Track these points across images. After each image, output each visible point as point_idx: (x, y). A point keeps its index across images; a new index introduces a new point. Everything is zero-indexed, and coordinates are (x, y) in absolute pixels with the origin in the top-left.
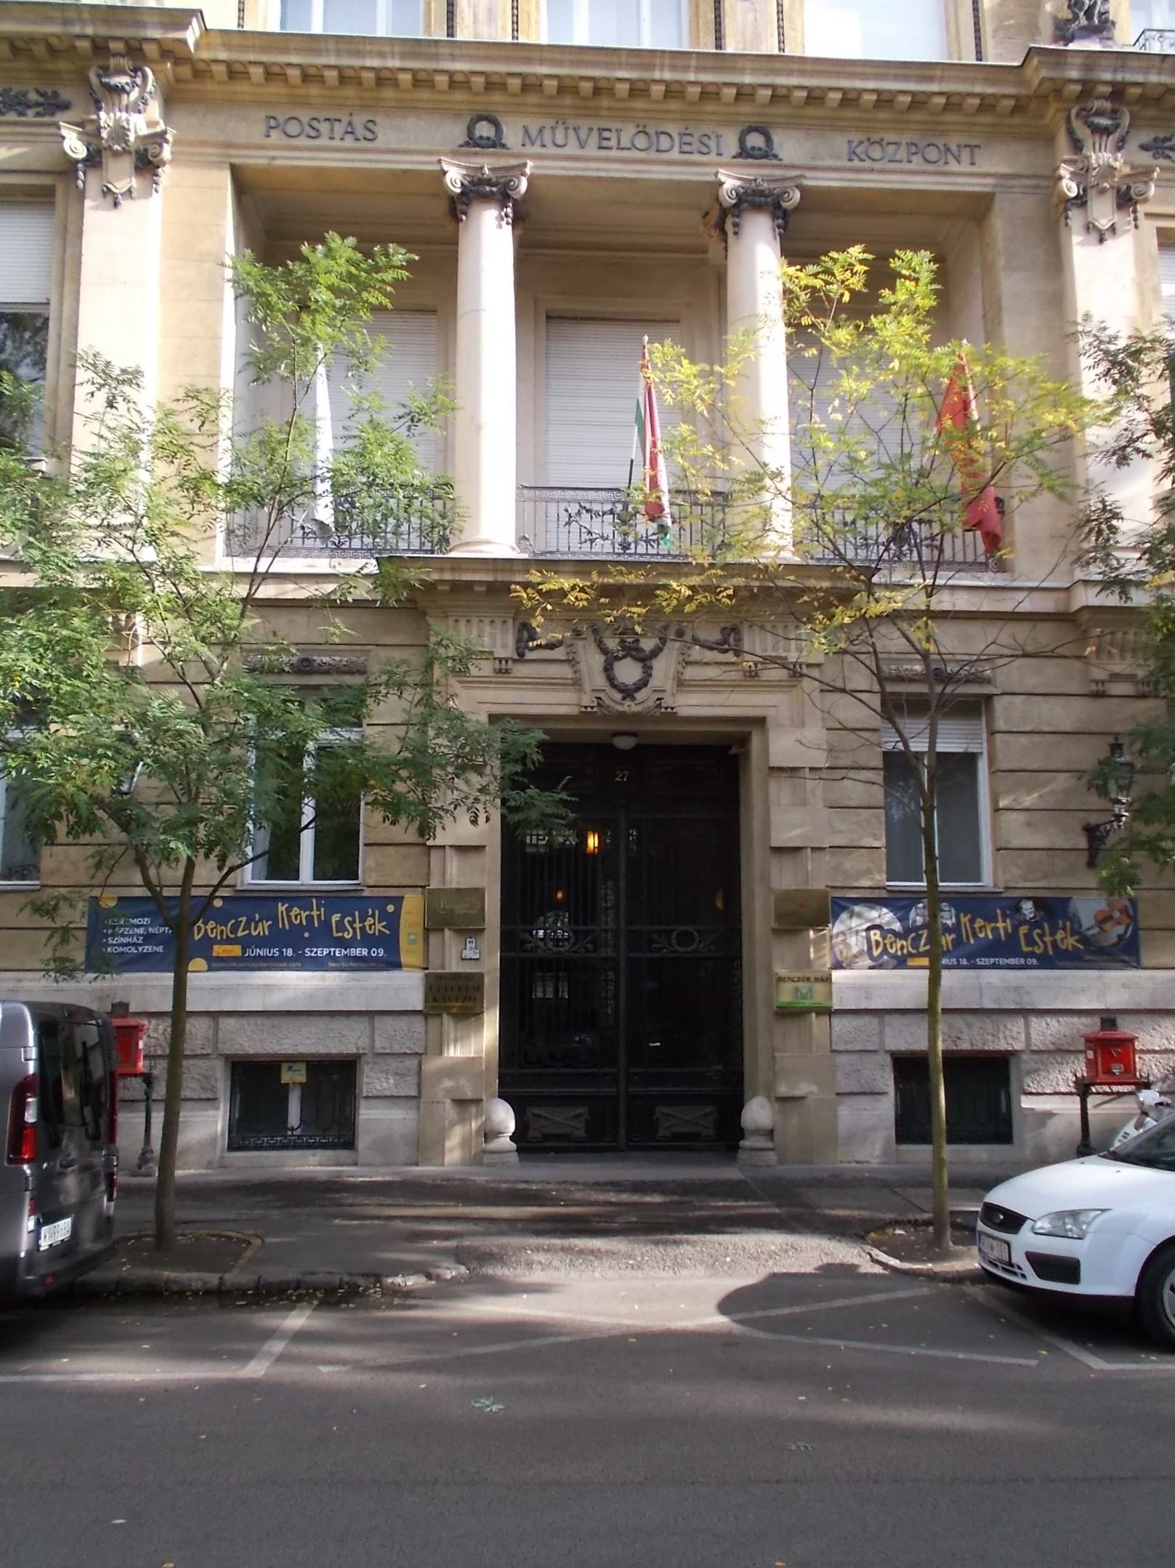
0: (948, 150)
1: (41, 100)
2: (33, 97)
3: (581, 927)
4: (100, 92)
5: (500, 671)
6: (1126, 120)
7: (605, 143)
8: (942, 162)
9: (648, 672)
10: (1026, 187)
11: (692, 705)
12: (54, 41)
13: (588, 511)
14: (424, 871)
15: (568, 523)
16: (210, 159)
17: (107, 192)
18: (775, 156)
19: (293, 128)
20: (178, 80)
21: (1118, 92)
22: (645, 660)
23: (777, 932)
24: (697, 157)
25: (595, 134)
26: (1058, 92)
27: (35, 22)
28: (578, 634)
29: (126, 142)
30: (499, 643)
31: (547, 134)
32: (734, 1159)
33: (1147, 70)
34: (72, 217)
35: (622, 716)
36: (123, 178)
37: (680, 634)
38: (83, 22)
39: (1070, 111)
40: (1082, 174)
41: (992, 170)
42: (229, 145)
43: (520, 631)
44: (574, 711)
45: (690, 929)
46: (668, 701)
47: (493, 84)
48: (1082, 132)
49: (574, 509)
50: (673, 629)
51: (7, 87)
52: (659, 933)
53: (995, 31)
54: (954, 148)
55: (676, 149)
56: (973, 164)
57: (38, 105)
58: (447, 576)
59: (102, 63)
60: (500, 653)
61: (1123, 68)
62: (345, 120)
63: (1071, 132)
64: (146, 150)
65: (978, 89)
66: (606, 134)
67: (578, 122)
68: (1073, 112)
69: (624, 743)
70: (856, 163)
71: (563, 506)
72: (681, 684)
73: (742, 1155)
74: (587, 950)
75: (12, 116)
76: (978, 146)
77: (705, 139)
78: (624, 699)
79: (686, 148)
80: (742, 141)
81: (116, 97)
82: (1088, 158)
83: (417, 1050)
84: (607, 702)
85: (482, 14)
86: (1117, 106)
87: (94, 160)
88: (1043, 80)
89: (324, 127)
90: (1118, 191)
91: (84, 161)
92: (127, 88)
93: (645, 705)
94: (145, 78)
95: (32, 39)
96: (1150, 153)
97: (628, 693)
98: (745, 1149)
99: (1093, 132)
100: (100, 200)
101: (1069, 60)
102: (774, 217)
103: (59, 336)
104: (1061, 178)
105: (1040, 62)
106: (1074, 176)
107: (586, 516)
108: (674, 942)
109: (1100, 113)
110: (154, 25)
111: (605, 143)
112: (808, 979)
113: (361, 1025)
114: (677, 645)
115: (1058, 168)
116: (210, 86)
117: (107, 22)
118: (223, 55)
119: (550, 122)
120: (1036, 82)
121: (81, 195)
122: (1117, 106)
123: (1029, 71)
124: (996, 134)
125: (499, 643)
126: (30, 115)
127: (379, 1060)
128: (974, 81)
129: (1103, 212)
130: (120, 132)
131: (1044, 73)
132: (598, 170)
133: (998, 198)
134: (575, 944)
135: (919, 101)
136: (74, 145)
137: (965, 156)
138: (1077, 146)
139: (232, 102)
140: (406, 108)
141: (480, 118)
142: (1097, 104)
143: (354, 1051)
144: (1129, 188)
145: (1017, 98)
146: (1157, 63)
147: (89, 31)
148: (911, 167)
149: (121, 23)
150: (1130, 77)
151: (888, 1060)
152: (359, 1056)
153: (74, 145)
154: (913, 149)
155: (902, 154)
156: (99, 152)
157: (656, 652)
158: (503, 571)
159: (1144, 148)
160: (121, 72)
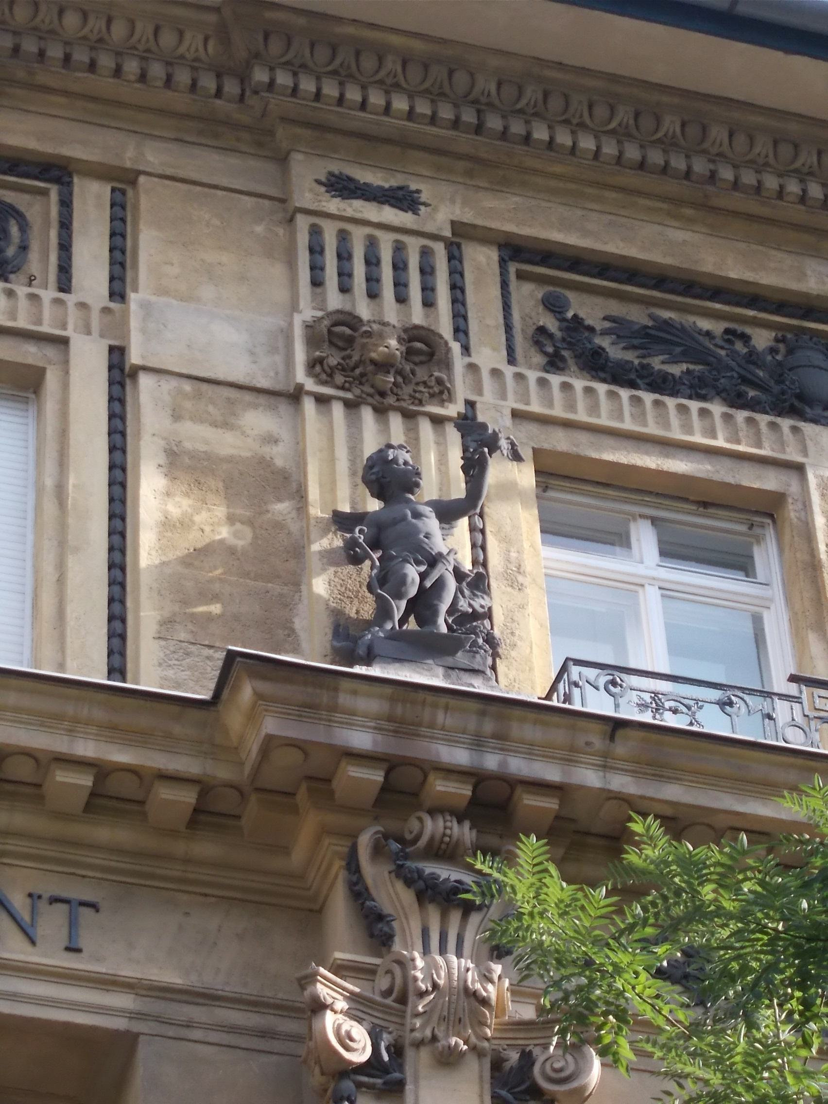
10: (233, 1029)
26: (321, 785)
33: (570, 756)
39: (353, 836)
40: (387, 1003)
41: (128, 972)
48: (392, 895)
53: (168, 623)
56: (73, 949)
63: (359, 893)
65: (86, 748)
68: (365, 841)
76: (93, 906)
82: (404, 964)
88: (269, 743)
90: (497, 1065)
99: (421, 897)
101: (344, 699)
104: (319, 1007)
105: (259, 696)
106: (359, 1007)
115: (311, 978)
120: (253, 747)
123: (234, 718)
124: (144, 879)
128: (74, 726)
131: (271, 725)
133: (144, 1052)
137: (52, 924)
138: (377, 930)
142: (432, 827)
144: (527, 1059)
145: (205, 787)
146: (596, 738)
150: (518, 765)
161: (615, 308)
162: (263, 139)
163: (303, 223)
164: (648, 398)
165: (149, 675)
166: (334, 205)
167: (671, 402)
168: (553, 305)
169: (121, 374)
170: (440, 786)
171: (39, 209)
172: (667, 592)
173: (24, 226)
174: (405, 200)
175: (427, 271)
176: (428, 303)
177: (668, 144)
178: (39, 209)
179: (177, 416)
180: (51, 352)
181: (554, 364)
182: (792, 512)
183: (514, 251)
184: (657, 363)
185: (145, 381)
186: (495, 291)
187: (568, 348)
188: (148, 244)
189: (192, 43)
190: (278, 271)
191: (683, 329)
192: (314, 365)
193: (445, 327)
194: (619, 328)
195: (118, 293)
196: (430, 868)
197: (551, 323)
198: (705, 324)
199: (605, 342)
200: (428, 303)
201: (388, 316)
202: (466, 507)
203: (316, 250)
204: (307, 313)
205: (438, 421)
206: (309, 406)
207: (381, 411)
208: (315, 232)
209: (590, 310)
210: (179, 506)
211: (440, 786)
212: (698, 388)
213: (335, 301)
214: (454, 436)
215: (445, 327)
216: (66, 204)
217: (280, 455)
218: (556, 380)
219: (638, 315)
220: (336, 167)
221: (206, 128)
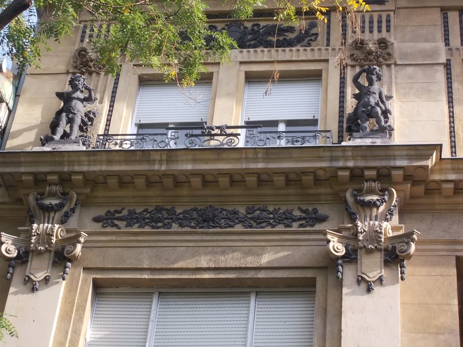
1: (304, 215)
2: (297, 213)
4: (353, 209)
12: (320, 173)
16: (440, 253)
17: (360, 280)
20: (412, 197)
27: (308, 161)
29: (379, 242)
34: (330, 301)
36: (372, 267)
38: (346, 159)
42: (455, 242)
51: (277, 207)
57: (300, 219)
59: (357, 186)
64: (394, 248)
75: (281, 228)
87: (351, 257)
91: (343, 257)
92: (378, 203)
94: (391, 195)
95: (304, 172)
100: (356, 287)
110: (402, 157)
116: (437, 199)
117: (365, 157)
118: (452, 177)
121: (340, 284)
126: (295, 226)
130: (375, 235)
136: (336, 246)
139: (454, 210)
147: (350, 164)
149: (375, 158)
153: (336, 246)
156: (355, 251)
160: (371, 192)
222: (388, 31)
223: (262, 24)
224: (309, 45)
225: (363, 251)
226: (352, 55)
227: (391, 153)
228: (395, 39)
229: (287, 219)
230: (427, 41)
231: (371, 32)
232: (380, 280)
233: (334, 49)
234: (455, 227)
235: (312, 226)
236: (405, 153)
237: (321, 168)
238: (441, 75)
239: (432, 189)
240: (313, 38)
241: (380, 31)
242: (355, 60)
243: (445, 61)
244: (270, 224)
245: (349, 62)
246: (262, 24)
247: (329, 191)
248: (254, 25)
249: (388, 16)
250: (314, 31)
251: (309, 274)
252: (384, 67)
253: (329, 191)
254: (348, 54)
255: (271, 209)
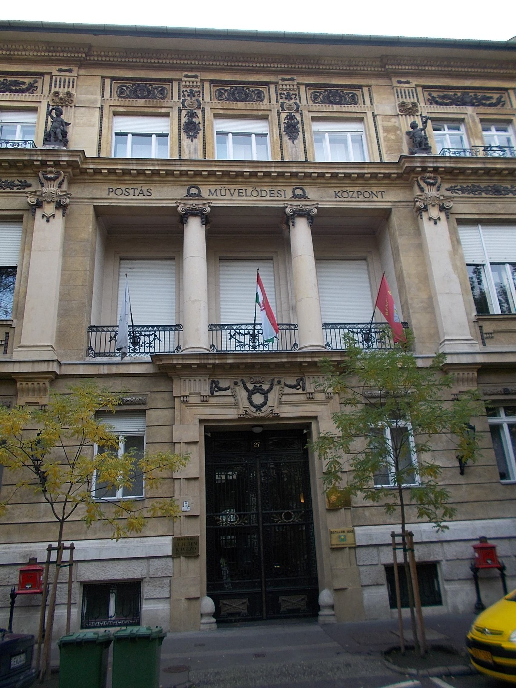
0: (372, 193)
1: (20, 183)
3: (242, 513)
4: (43, 180)
5: (203, 401)
6: (439, 180)
7: (241, 194)
8: (371, 197)
9: (266, 399)
11: (286, 412)
12: (26, 162)
13: (238, 333)
14: (172, 490)
15: (230, 339)
18: (307, 197)
19: (119, 192)
20: (74, 175)
21: (436, 170)
22: (265, 394)
23: (329, 510)
24: (277, 198)
25: (237, 191)
28: (236, 383)
30: (202, 389)
31: (218, 192)
32: (317, 621)
35: (256, 419)
37: (279, 382)
41: (390, 200)
43: (212, 384)
44: (236, 417)
45: (290, 511)
46: (276, 411)
47: (198, 174)
48: (423, 185)
49: (233, 332)
50: (276, 380)
52: (276, 514)
53: (387, 151)
54: (375, 193)
55: (268, 196)
58: (181, 362)
59: (44, 170)
60: (203, 393)
61: (436, 162)
62: (139, 189)
63: (419, 185)
65: (382, 171)
66: (241, 191)
67: (230, 187)
68: (419, 178)
69: (258, 430)
70: (338, 199)
71: (228, 332)
72: (280, 403)
73: (320, 619)
74: (245, 523)
75: (8, 190)
77: (279, 192)
78: (256, 411)
79: (272, 195)
80: (293, 192)
81: (49, 182)
83: (169, 575)
84: (249, 412)
85: (192, 151)
86: (435, 176)
89: (131, 192)
90: (439, 205)
93: (266, 413)
96: (450, 192)
97: (258, 408)
98: (321, 615)
99: (427, 185)
102: (308, 219)
103: (22, 271)
107: (237, 336)
108: (283, 517)
109: (429, 178)
111: (241, 194)
112: (344, 532)
113: (144, 563)
114: (278, 387)
119: (220, 187)
122: (435, 176)
125: (202, 389)
127: (152, 580)
129: (434, 212)
131: (406, 165)
132: (238, 204)
133: (393, 209)
134: (239, 521)
135: (361, 176)
137: (379, 195)
140: (163, 183)
141: (192, 187)
143: (140, 576)
144: (443, 204)
147: (40, 158)
148: (358, 200)
150: (439, 165)
151: (383, 568)
152: (142, 579)
154: (359, 193)
155: (355, 195)
157: (269, 391)
158: (204, 359)
159: (447, 190)
160: (51, 172)
161: (438, 93)
162: (387, 75)
163: (395, 88)
164: (445, 106)
165: (386, 160)
166: (399, 85)
167: (448, 107)
168: (430, 95)
169: (374, 116)
170: (429, 169)
171: (359, 93)
172: (450, 135)
173: (357, 96)
174: (408, 82)
175: (412, 93)
176: (413, 98)
177: (445, 66)
178: (359, 93)
179: (383, 121)
180: (364, 114)
181: (431, 104)
182: (466, 120)
183: (424, 87)
184: (445, 101)
185: (377, 116)
186: (422, 94)
187: (433, 101)
188: (375, 96)
189: (377, 63)
190: (393, 97)
191: (448, 95)
192: (400, 110)
193: (416, 101)
194: (440, 97)
195: (372, 104)
196: (428, 181)
197: (429, 97)
198: (451, 93)
199: (437, 99)
200: (413, 98)
201: (409, 101)
202: (423, 129)
203: (397, 93)
204: (398, 103)
205: (417, 115)
206: (400, 116)
207: (409, 115)
208: (397, 90)
209: (435, 94)
210: (385, 134)
211: (429, 169)
212: (451, 104)
213: (401, 100)
214: (419, 116)
215: (416, 101)
216: (362, 92)
217: (397, 124)
218: (432, 106)
219: (441, 94)
220: (398, 79)
221: (379, 76)
222: (73, 87)
223: (9, 79)
224: (33, 93)
225: (45, 202)
226: (53, 100)
227: (60, 153)
228: (76, 92)
229: (11, 185)
230: (92, 94)
231: (64, 87)
232: (53, 216)
233: (44, 96)
234: (94, 191)
235: (24, 189)
236: (66, 153)
237: (25, 160)
238: (97, 113)
239: (84, 172)
240: (35, 89)
241: (68, 87)
242: (54, 102)
243: (100, 106)
244: (2, 188)
245: (51, 103)
246: (9, 79)
247: (32, 171)
248: (4, 80)
249: (74, 79)
250: (35, 85)
251: (20, 213)
252: (69, 107)
253: (32, 171)
254: (51, 99)
255: (3, 180)
